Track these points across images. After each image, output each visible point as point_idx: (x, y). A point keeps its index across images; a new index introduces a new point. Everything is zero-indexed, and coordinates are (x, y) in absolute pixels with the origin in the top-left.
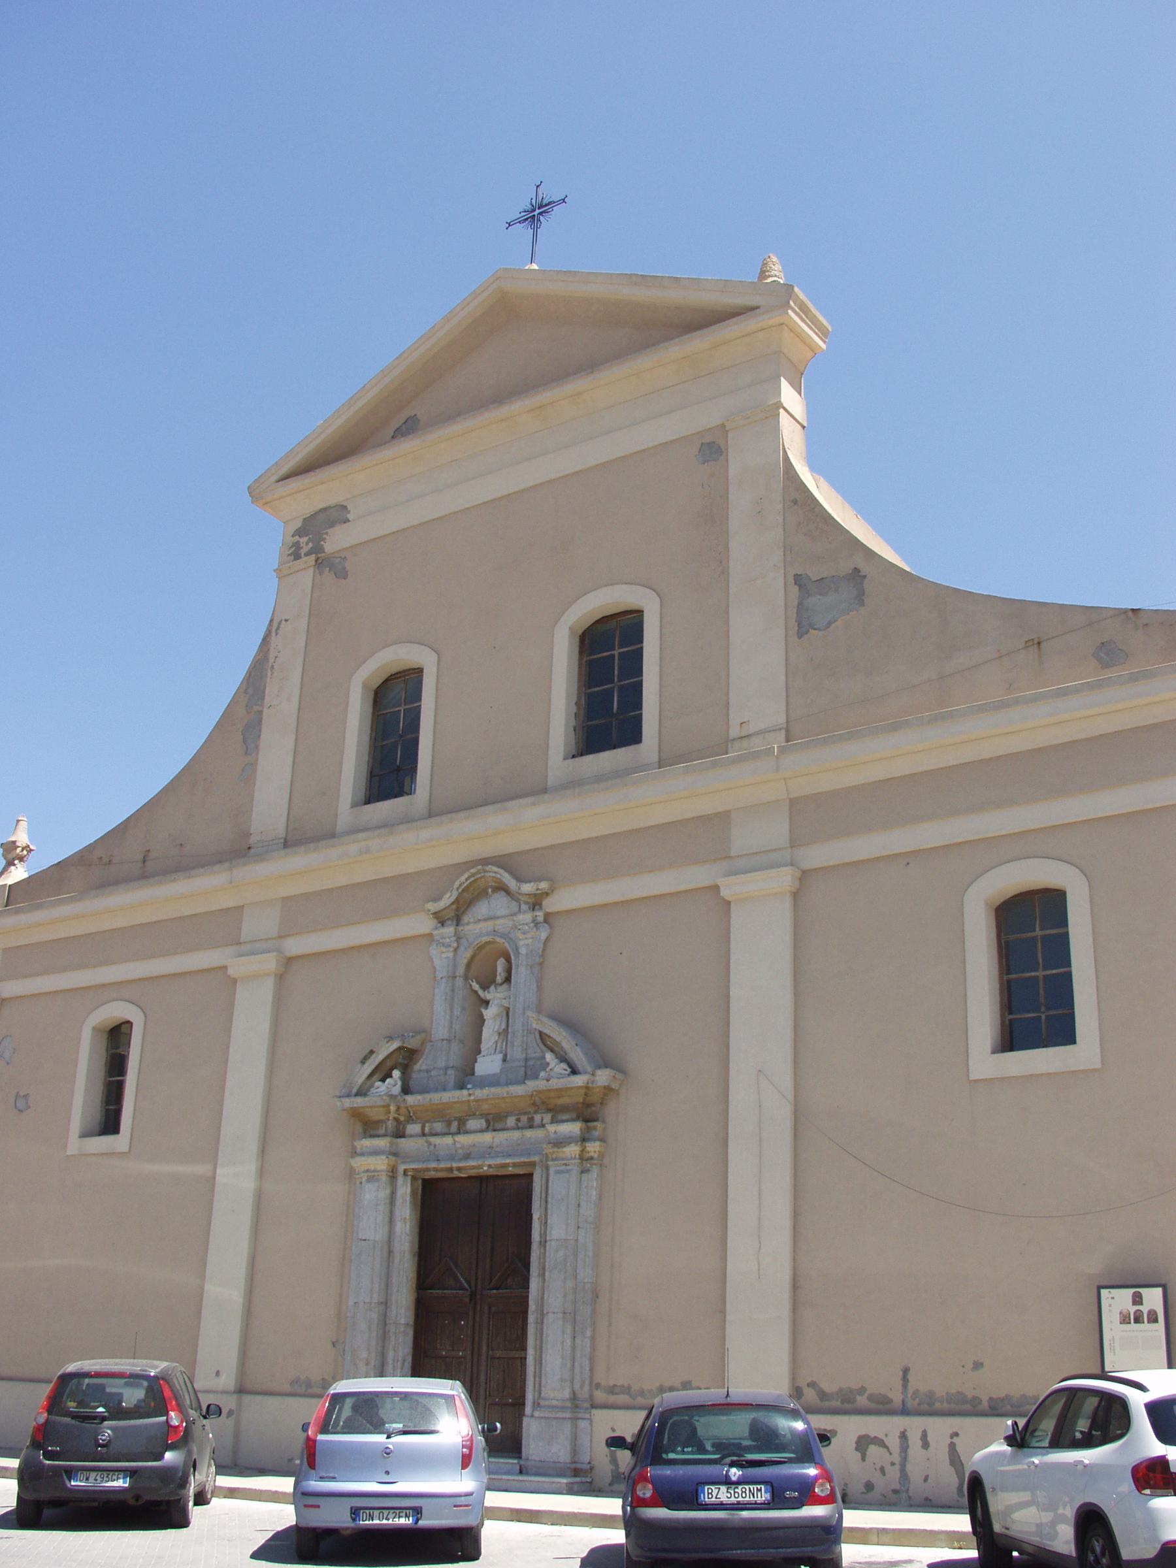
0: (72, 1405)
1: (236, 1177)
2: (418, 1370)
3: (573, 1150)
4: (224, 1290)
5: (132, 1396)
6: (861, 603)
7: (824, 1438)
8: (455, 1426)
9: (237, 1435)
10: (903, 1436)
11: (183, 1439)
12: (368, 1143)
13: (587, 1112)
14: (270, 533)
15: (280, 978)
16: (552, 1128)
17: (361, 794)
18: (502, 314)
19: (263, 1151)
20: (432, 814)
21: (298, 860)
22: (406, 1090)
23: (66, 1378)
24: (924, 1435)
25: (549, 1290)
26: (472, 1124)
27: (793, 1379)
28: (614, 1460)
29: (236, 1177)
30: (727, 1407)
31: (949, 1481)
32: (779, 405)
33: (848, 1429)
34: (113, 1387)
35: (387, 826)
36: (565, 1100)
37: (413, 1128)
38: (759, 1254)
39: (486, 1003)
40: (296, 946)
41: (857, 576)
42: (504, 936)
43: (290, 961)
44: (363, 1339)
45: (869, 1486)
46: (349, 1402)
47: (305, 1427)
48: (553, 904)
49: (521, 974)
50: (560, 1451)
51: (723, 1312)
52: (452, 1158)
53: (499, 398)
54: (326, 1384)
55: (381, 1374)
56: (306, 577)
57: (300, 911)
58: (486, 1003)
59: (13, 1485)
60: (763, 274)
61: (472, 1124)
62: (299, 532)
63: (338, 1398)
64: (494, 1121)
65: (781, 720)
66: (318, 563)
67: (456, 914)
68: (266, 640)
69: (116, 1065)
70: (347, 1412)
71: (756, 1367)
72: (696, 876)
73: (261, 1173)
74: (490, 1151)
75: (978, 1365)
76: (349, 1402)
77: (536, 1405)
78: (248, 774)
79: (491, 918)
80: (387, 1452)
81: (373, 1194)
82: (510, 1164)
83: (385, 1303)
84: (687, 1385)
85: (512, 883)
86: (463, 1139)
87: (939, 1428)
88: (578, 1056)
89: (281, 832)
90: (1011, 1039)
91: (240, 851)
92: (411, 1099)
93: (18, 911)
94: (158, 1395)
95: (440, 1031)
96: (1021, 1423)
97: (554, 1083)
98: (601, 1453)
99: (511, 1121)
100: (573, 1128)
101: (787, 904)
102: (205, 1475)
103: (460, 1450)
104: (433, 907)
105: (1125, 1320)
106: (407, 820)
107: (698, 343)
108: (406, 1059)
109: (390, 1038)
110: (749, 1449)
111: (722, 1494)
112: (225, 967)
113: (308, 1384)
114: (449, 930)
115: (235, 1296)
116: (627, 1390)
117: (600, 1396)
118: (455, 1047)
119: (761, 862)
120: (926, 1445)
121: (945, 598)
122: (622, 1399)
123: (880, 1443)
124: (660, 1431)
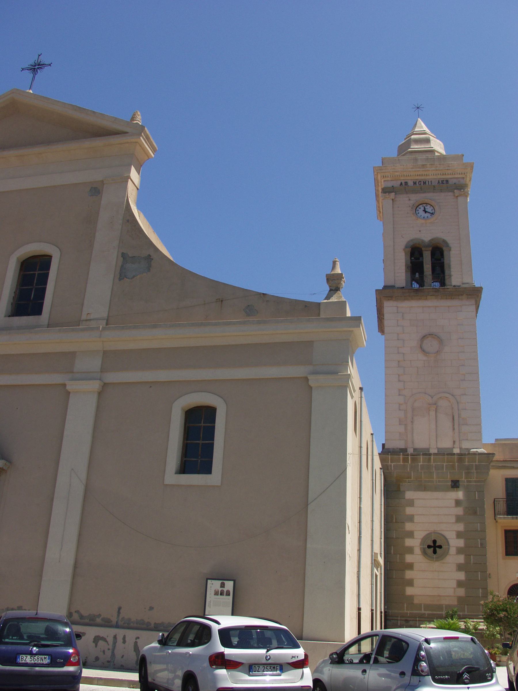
6: (149, 270)
7: (79, 636)
10: (115, 637)
24: (124, 637)
27: (69, 608)
30: (36, 619)
31: (133, 658)
32: (129, 177)
33: (91, 632)
38: (61, 552)
41: (149, 258)
45: (97, 659)
51: (41, 576)
60: (133, 118)
65: (105, 315)
71: (53, 602)
72: (56, 379)
75: (151, 608)
84: (20, 608)
87: (131, 635)
90: (185, 468)
96: (166, 634)
101: (96, 396)
105: (216, 593)
107: (98, 143)
110: (43, 639)
119: (87, 376)
120: (124, 642)
121: (186, 275)
123: (105, 640)
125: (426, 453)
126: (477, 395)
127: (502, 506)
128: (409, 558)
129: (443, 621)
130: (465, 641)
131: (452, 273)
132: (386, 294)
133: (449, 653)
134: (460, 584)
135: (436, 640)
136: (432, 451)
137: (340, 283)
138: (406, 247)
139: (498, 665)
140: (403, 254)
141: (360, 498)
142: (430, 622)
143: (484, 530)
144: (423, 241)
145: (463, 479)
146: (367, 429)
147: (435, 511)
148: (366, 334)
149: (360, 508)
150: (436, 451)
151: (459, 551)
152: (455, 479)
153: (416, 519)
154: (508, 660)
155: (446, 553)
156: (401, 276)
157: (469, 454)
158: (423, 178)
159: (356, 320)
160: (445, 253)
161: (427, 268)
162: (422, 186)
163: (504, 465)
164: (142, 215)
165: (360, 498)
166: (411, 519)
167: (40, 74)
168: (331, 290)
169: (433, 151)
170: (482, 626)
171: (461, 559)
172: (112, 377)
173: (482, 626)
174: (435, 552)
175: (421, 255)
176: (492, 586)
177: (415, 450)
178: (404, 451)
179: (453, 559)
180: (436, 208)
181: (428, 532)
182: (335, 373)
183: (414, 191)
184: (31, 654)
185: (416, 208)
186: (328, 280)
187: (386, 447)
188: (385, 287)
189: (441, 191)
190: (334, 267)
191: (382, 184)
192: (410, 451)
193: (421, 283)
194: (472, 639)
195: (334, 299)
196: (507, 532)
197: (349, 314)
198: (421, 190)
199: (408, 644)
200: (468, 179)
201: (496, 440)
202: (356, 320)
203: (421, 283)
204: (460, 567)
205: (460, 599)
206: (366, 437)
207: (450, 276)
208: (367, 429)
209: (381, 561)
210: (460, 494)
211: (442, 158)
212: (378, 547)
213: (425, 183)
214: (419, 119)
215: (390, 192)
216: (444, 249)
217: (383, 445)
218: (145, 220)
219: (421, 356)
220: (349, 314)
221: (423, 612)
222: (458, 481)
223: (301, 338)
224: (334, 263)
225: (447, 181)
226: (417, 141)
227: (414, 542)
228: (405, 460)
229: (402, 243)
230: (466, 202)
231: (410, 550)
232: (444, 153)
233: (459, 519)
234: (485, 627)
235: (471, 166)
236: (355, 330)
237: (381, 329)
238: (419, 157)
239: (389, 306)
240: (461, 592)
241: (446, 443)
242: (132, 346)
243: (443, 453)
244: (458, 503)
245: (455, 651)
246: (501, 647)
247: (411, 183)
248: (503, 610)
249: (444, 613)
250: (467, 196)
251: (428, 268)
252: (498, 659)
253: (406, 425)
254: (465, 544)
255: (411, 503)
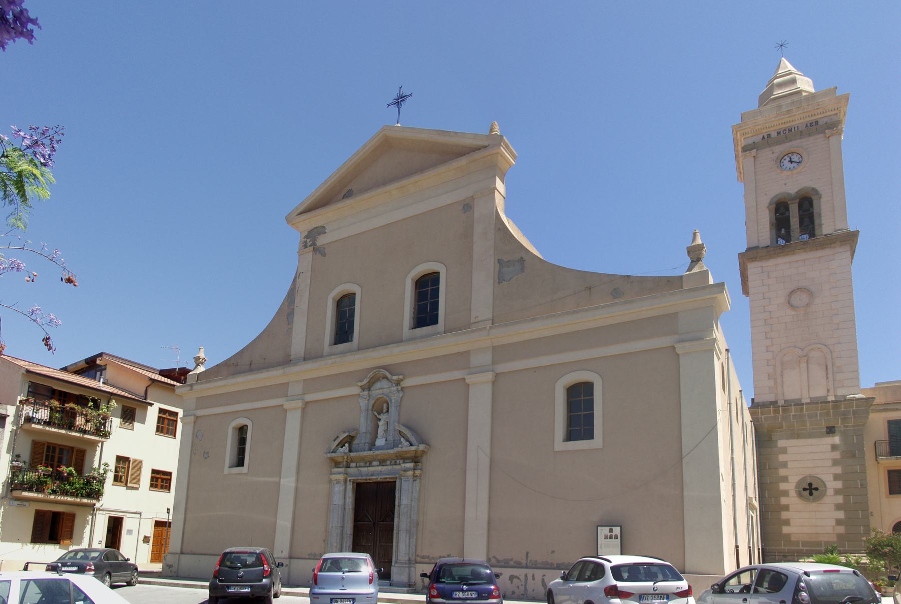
0: (228, 563)
1: (288, 482)
2: (354, 550)
3: (410, 473)
4: (284, 522)
5: (251, 560)
6: (523, 271)
7: (497, 576)
8: (367, 569)
9: (289, 573)
10: (526, 575)
11: (270, 575)
12: (336, 470)
13: (416, 459)
14: (294, 237)
15: (304, 410)
16: (403, 465)
17: (333, 341)
18: (386, 145)
19: (298, 472)
20: (359, 349)
21: (309, 366)
22: (350, 451)
23: (226, 554)
24: (533, 576)
25: (401, 522)
26: (375, 463)
27: (488, 555)
28: (423, 582)
29: (288, 482)
30: (463, 564)
31: (542, 591)
32: (495, 188)
33: (506, 573)
34: (243, 557)
35: (343, 353)
36: (408, 455)
37: (353, 465)
38: (477, 513)
39: (380, 420)
40: (309, 398)
41: (522, 260)
42: (387, 395)
43: (307, 403)
44: (334, 540)
45: (513, 593)
46: (329, 561)
47: (313, 570)
48: (403, 384)
49: (392, 409)
50: (404, 578)
51: (463, 531)
52: (367, 475)
53: (385, 182)
54: (321, 555)
55: (341, 551)
56: (309, 255)
57: (311, 384)
58: (380, 420)
59: (207, 591)
60: (491, 130)
61: (375, 463)
62: (306, 237)
63: (325, 560)
64: (382, 462)
65: (490, 316)
66: (315, 250)
67: (368, 387)
68: (295, 280)
69: (242, 441)
70: (329, 565)
71: (475, 552)
72: (457, 375)
73: (297, 481)
74: (381, 473)
75: (553, 552)
76: (329, 561)
77: (396, 562)
78: (289, 333)
79: (381, 389)
80: (343, 578)
81: (338, 488)
82: (387, 477)
83: (343, 527)
84: (449, 556)
85: (389, 376)
86: (371, 469)
87: (538, 573)
88: (413, 439)
89: (303, 355)
90: (570, 436)
91: (287, 361)
92: (352, 454)
93: (202, 383)
94: (260, 559)
95: (363, 429)
96: (567, 572)
97: (404, 449)
98: (419, 579)
99: (388, 462)
100: (411, 465)
101: (490, 385)
102: (277, 588)
103: (369, 578)
104: (360, 384)
105: (606, 537)
106: (350, 351)
107: (463, 161)
108: (350, 439)
109: (344, 432)
110: (470, 579)
111: (461, 595)
112: (282, 406)
113: (315, 555)
114: (366, 393)
115: (289, 524)
116: (428, 557)
117: (418, 559)
118: (368, 436)
119: (481, 370)
120: (534, 579)
121: (556, 270)
122: (426, 560)
123: (518, 578)
124: (439, 571)
125: (798, 404)
126: (853, 342)
127: (884, 447)
128: (784, 501)
129: (823, 556)
130: (848, 574)
131: (823, 222)
132: (751, 255)
133: (830, 584)
134: (839, 522)
135: (815, 573)
136: (804, 401)
137: (701, 253)
138: (770, 204)
139: (883, 596)
140: (767, 212)
141: (732, 449)
142: (808, 557)
143: (864, 471)
144: (789, 194)
145: (839, 424)
146: (736, 386)
147: (809, 456)
148: (730, 298)
149: (732, 458)
150: (808, 401)
151: (837, 492)
152: (831, 424)
153: (790, 465)
154: (895, 591)
155: (824, 494)
156: (765, 235)
157: (845, 400)
158: (788, 125)
159: (720, 286)
160: (815, 202)
161: (795, 221)
162: (787, 134)
163: (885, 407)
164: (511, 222)
165: (732, 449)
166: (785, 465)
167: (404, 105)
168: (692, 262)
169: (799, 92)
170: (865, 560)
171: (840, 499)
172: (502, 368)
173: (865, 560)
174: (811, 494)
175: (787, 208)
176: (874, 522)
177: (786, 401)
178: (774, 403)
179: (831, 499)
180: (804, 155)
181: (801, 477)
182: (701, 339)
183: (778, 142)
184: (462, 590)
185: (780, 160)
186: (688, 252)
187: (756, 401)
188: (748, 249)
189: (810, 135)
190: (694, 239)
191: (742, 143)
192: (781, 403)
193: (788, 238)
194: (854, 572)
195: (696, 270)
196: (891, 473)
197: (711, 282)
198: (787, 139)
199: (787, 577)
200: (842, 114)
201: (877, 384)
202: (720, 286)
203: (788, 238)
204: (838, 507)
205: (839, 536)
206: (735, 393)
207: (821, 225)
208: (736, 386)
209: (756, 504)
210: (836, 440)
211: (811, 97)
212: (753, 492)
213: (790, 130)
214: (783, 59)
215: (750, 150)
216: (814, 198)
217: (753, 400)
218: (515, 226)
219: (790, 312)
220: (711, 282)
221: (801, 548)
222: (834, 427)
223: (669, 311)
224: (695, 235)
225: (817, 123)
226: (780, 85)
227: (790, 486)
228: (776, 412)
229: (765, 200)
230: (840, 141)
231: (785, 493)
232: (812, 90)
233: (835, 463)
234: (868, 561)
235: (846, 98)
236: (719, 296)
237: (746, 291)
238: (783, 102)
239: (753, 268)
240: (841, 529)
241: (819, 392)
242: (515, 339)
243: (815, 402)
244: (834, 447)
245: (837, 583)
246: (886, 579)
247: (774, 135)
248: (888, 545)
249: (823, 549)
250: (840, 134)
251: (795, 221)
252: (883, 590)
253: (775, 380)
254: (843, 485)
255: (784, 451)
